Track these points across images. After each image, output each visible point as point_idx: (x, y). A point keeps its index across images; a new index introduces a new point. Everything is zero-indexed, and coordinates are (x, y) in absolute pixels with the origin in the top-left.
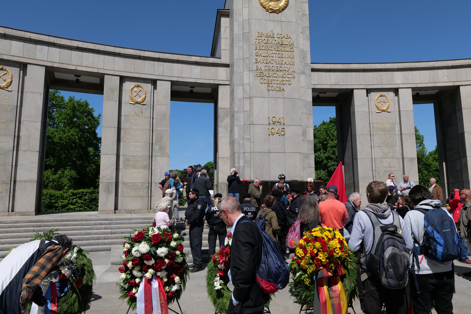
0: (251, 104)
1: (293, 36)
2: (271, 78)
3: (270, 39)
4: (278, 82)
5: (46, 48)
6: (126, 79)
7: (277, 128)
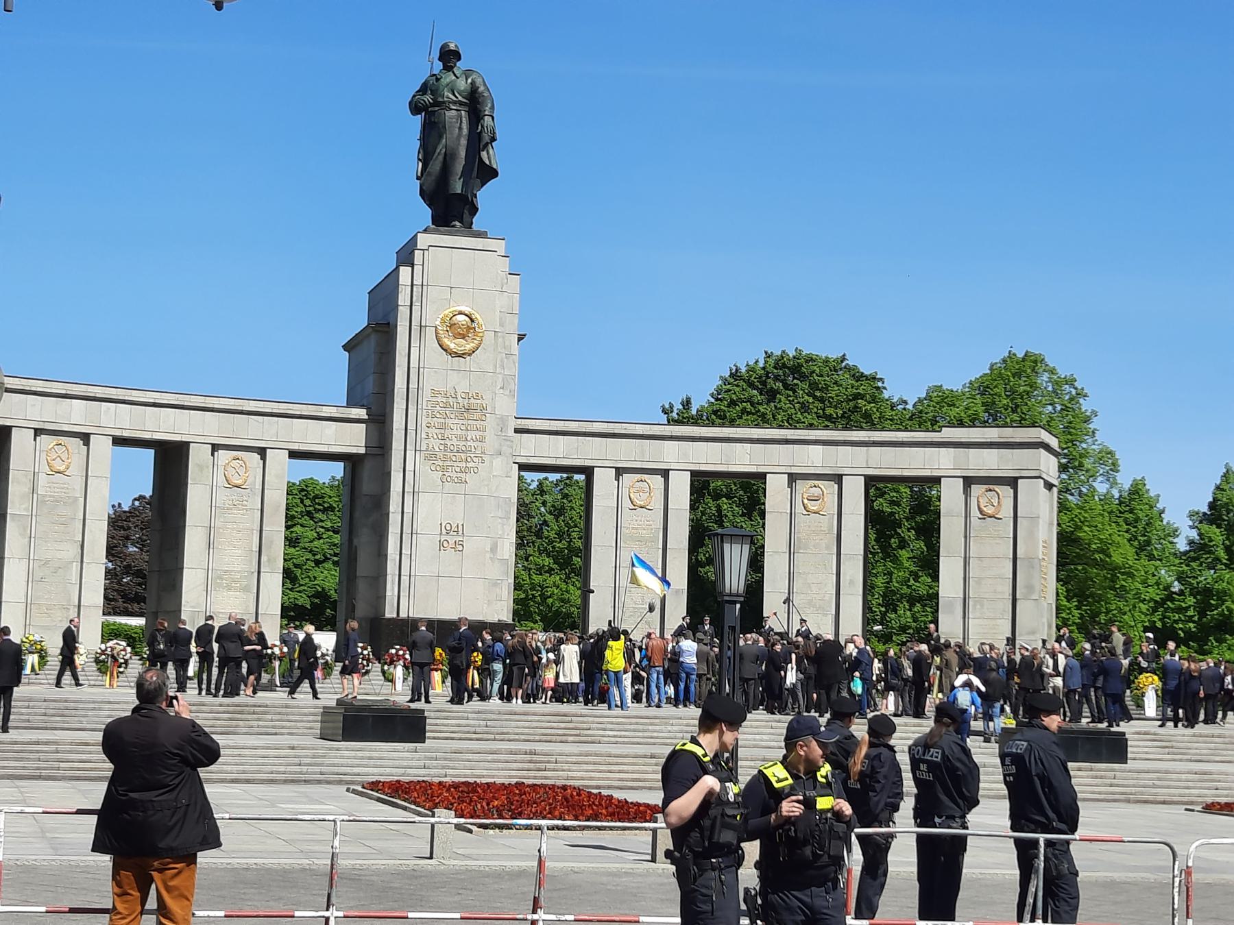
1: (487, 397)
2: (449, 463)
3: (451, 400)
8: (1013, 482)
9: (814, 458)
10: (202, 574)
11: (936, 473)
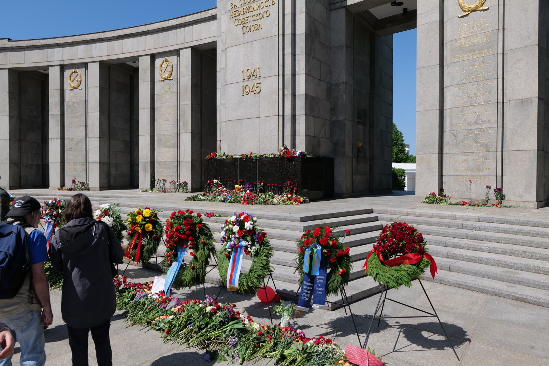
0: (226, 56)
4: (254, 18)
6: (156, 56)
7: (250, 84)
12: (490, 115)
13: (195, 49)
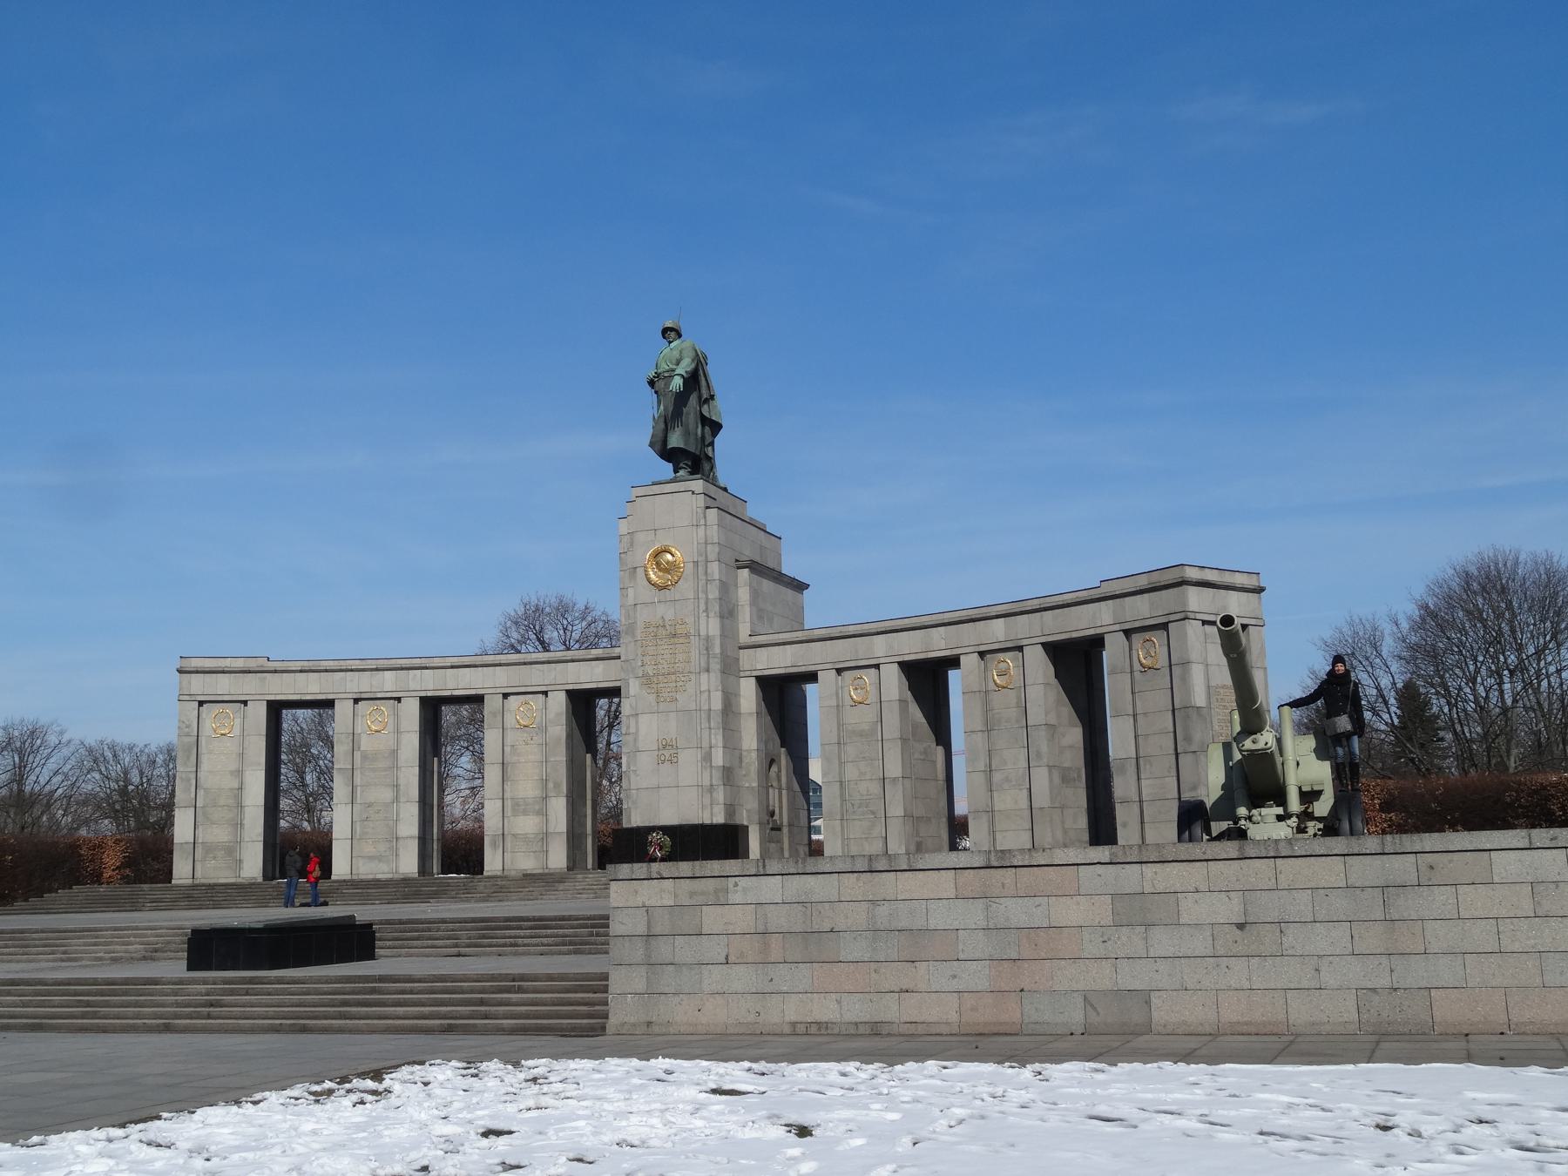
5: (418, 672)
7: (667, 753)
8: (1164, 626)
9: (997, 632)
10: (499, 803)
11: (1099, 631)
12: (875, 788)
13: (571, 694)
